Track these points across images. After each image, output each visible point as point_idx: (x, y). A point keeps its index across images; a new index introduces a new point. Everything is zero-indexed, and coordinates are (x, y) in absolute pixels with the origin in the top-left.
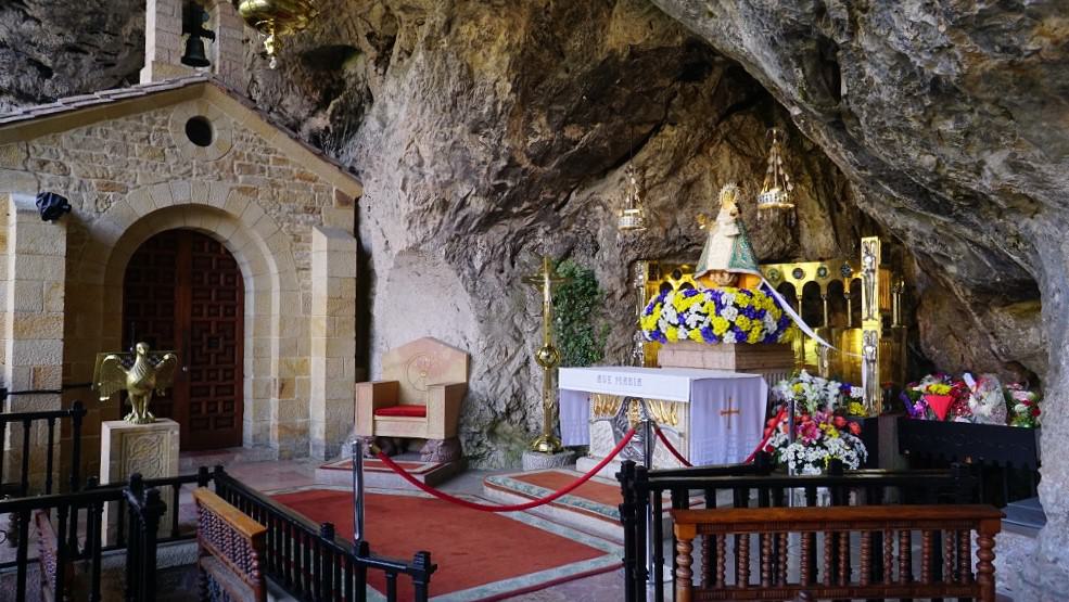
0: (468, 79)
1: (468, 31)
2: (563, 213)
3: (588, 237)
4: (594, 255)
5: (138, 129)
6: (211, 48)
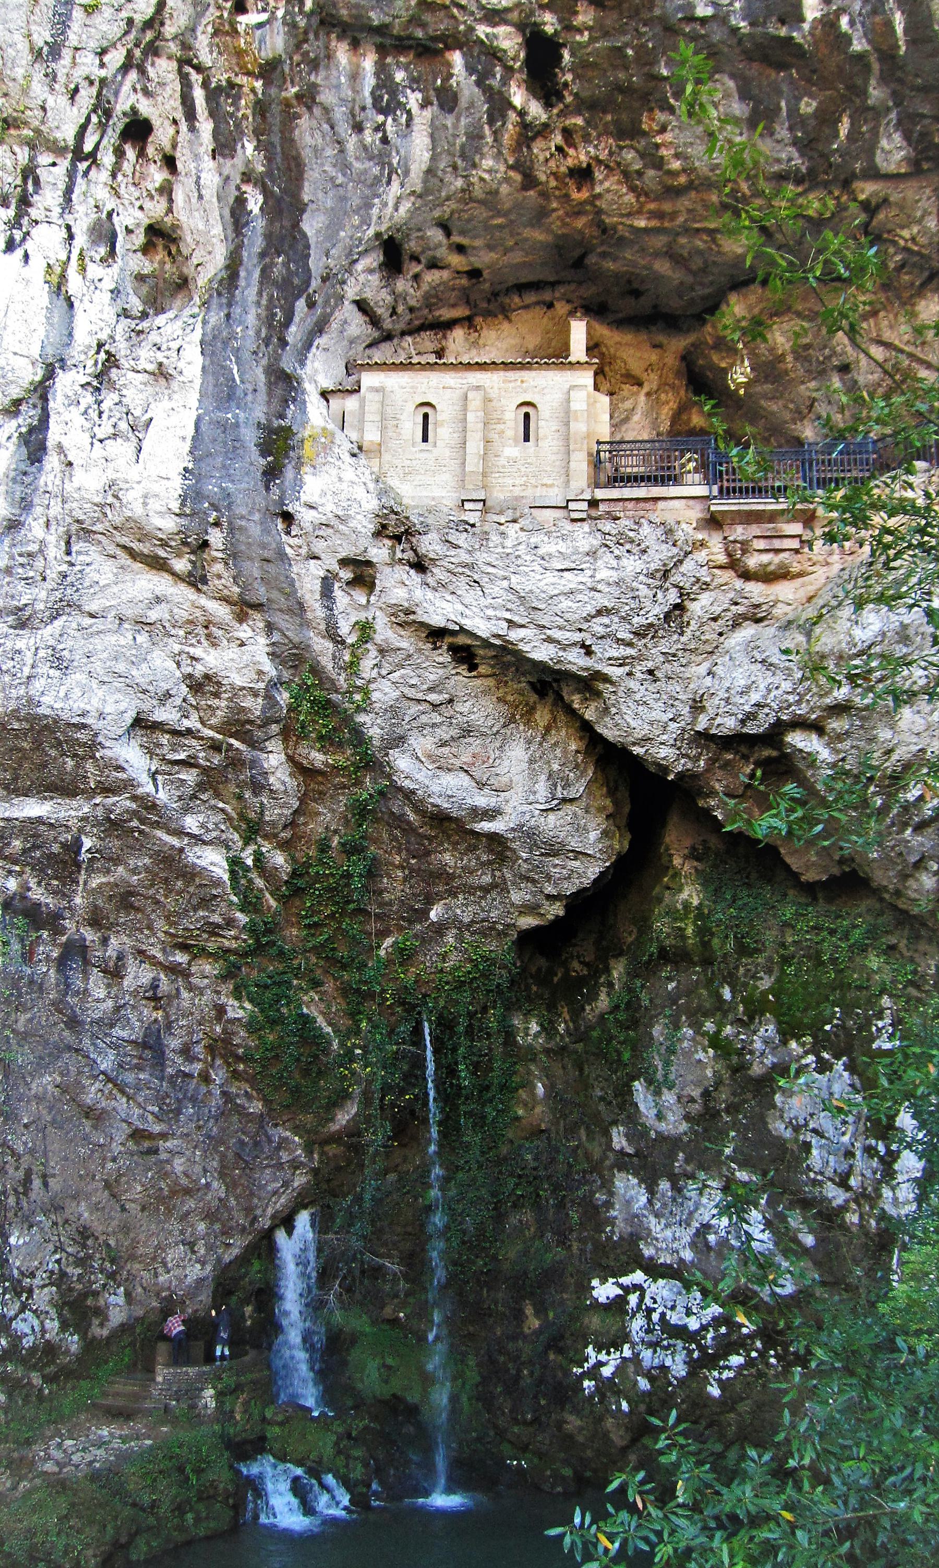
1: (663, 397)
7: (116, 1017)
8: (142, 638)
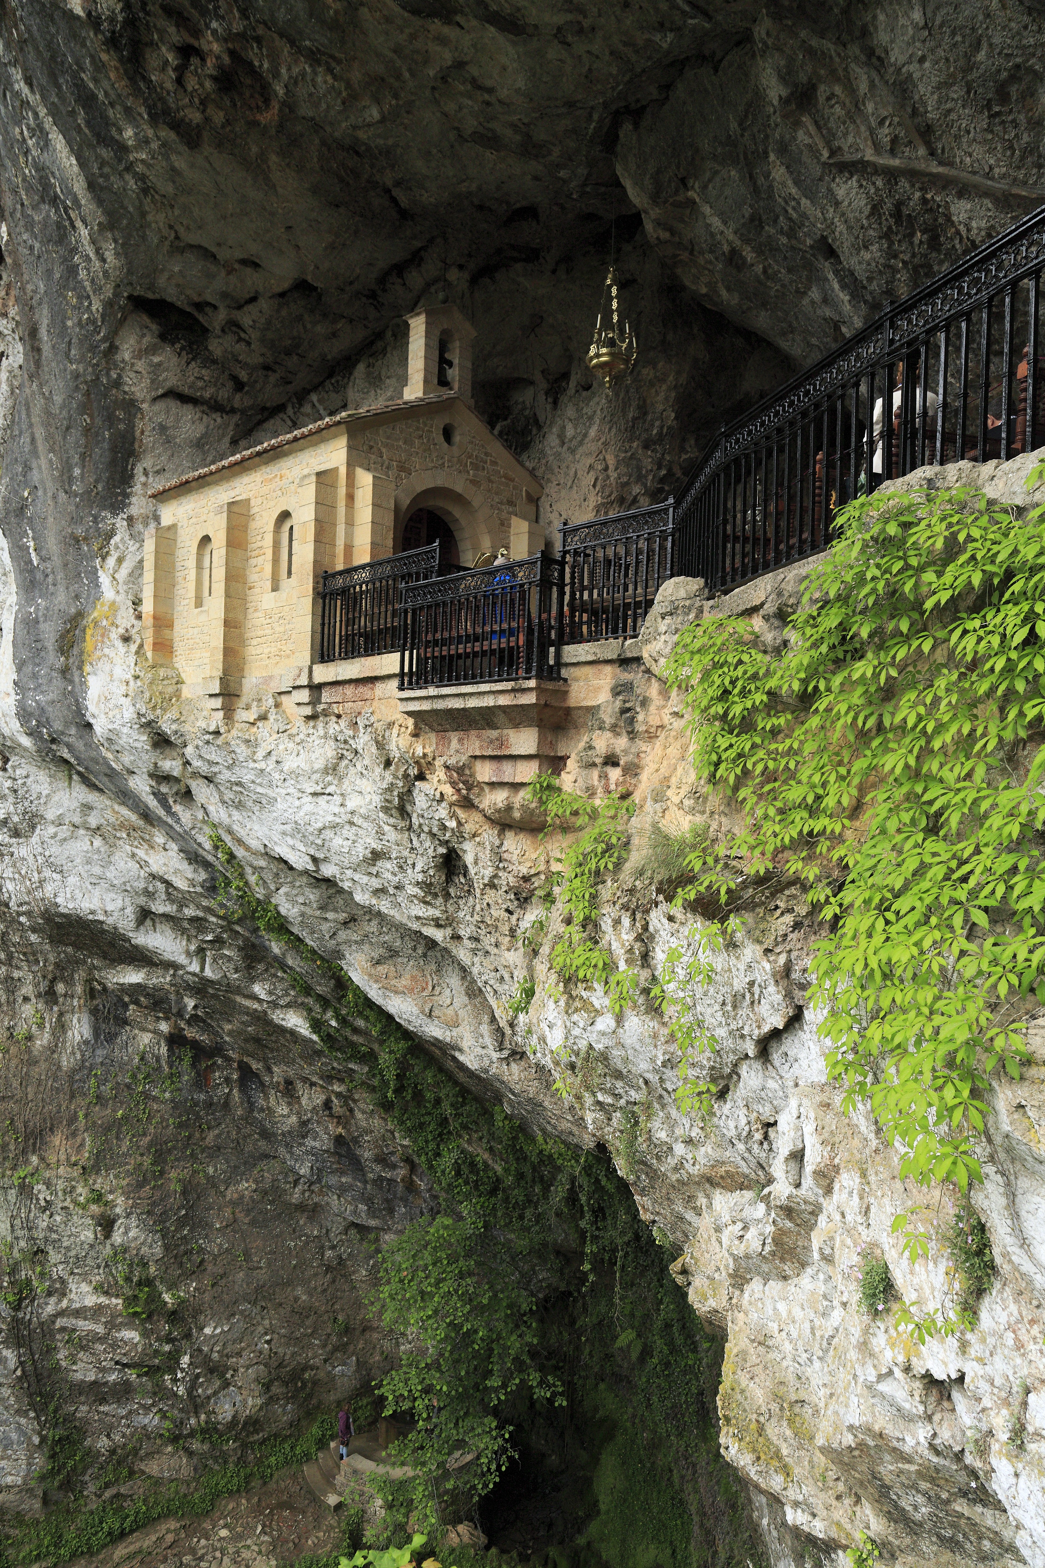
0: (643, 410)
5: (418, 429)
6: (453, 373)
7: (304, 1129)
8: (98, 842)
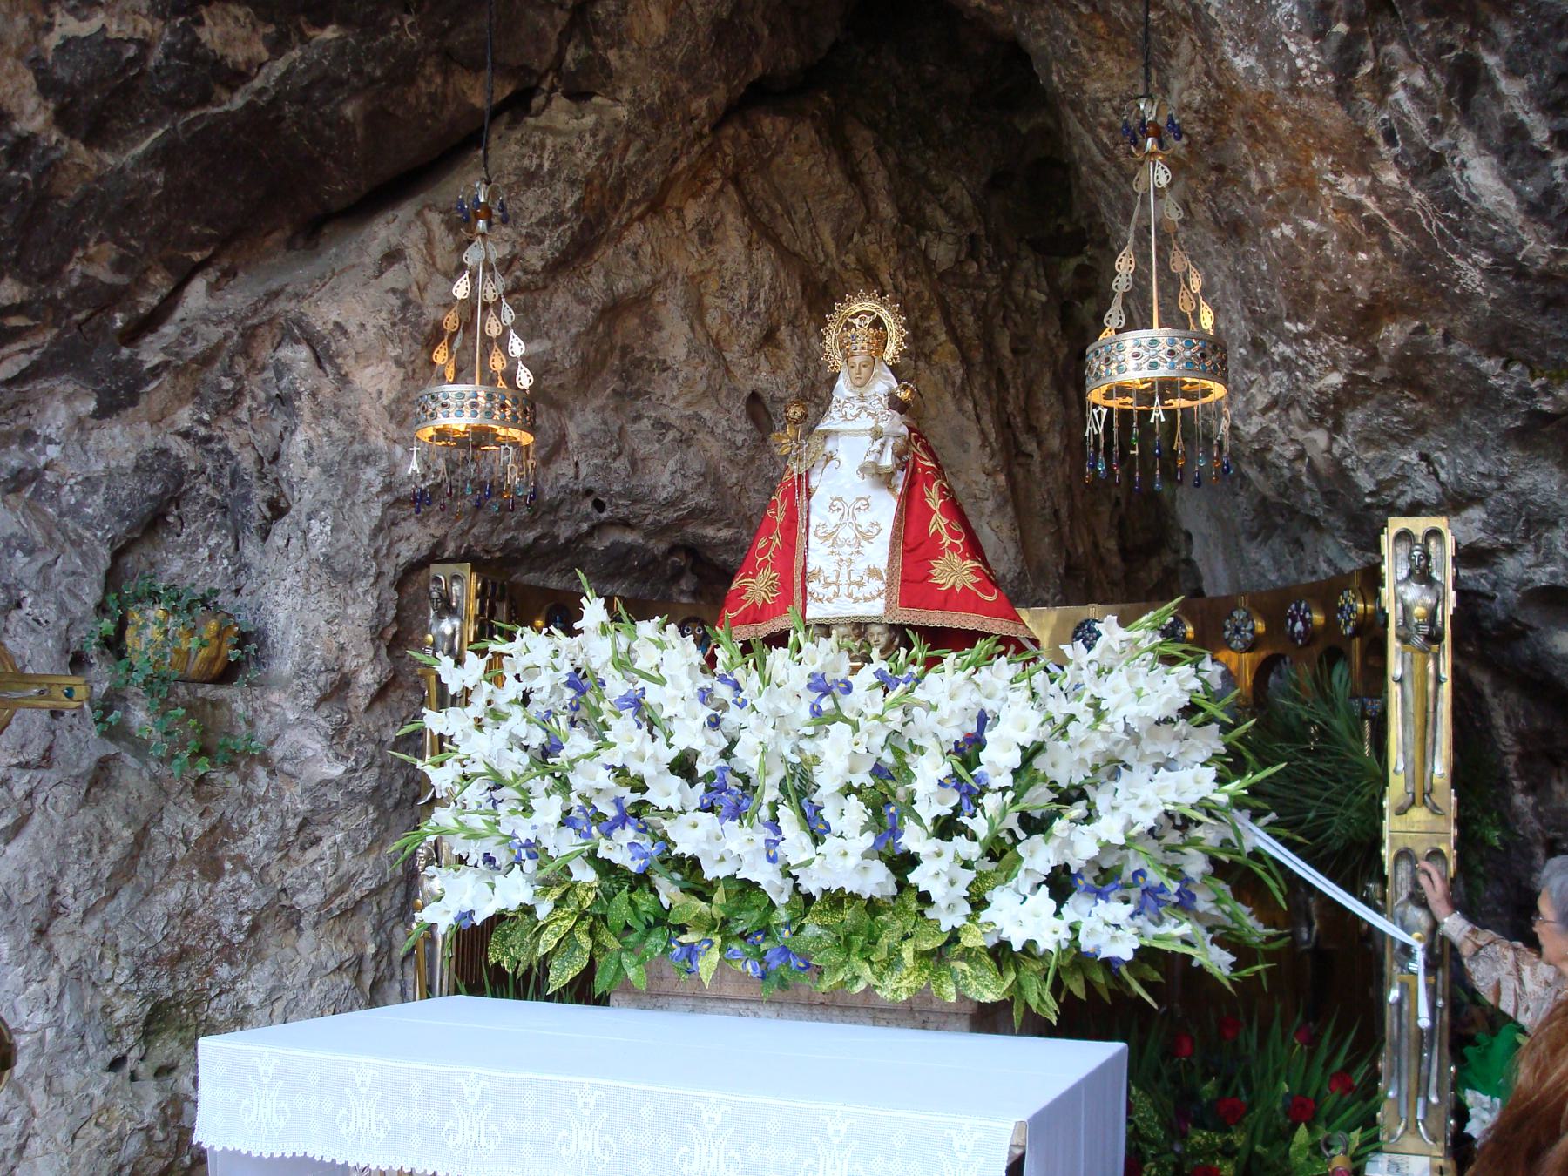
2: (150, 353)
3: (247, 460)
4: (265, 534)
